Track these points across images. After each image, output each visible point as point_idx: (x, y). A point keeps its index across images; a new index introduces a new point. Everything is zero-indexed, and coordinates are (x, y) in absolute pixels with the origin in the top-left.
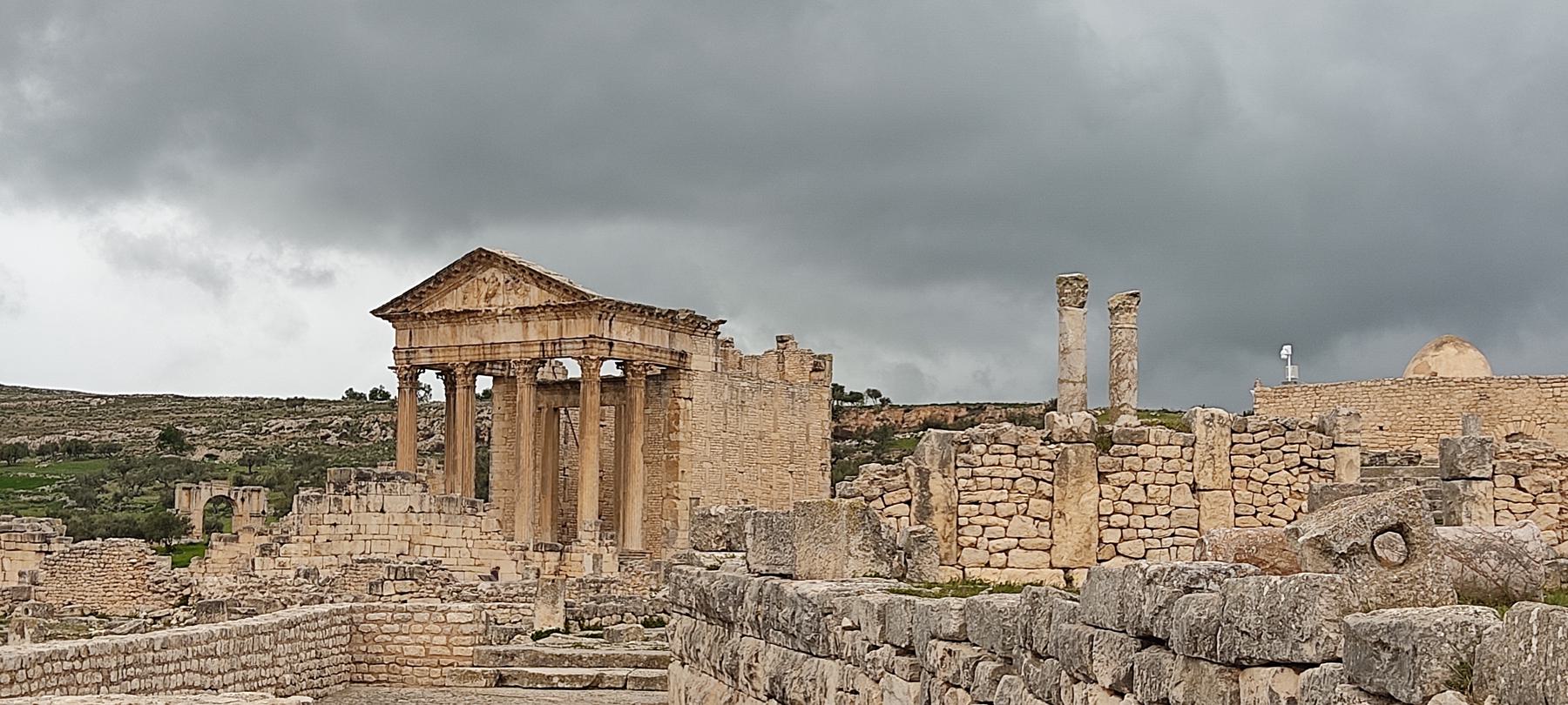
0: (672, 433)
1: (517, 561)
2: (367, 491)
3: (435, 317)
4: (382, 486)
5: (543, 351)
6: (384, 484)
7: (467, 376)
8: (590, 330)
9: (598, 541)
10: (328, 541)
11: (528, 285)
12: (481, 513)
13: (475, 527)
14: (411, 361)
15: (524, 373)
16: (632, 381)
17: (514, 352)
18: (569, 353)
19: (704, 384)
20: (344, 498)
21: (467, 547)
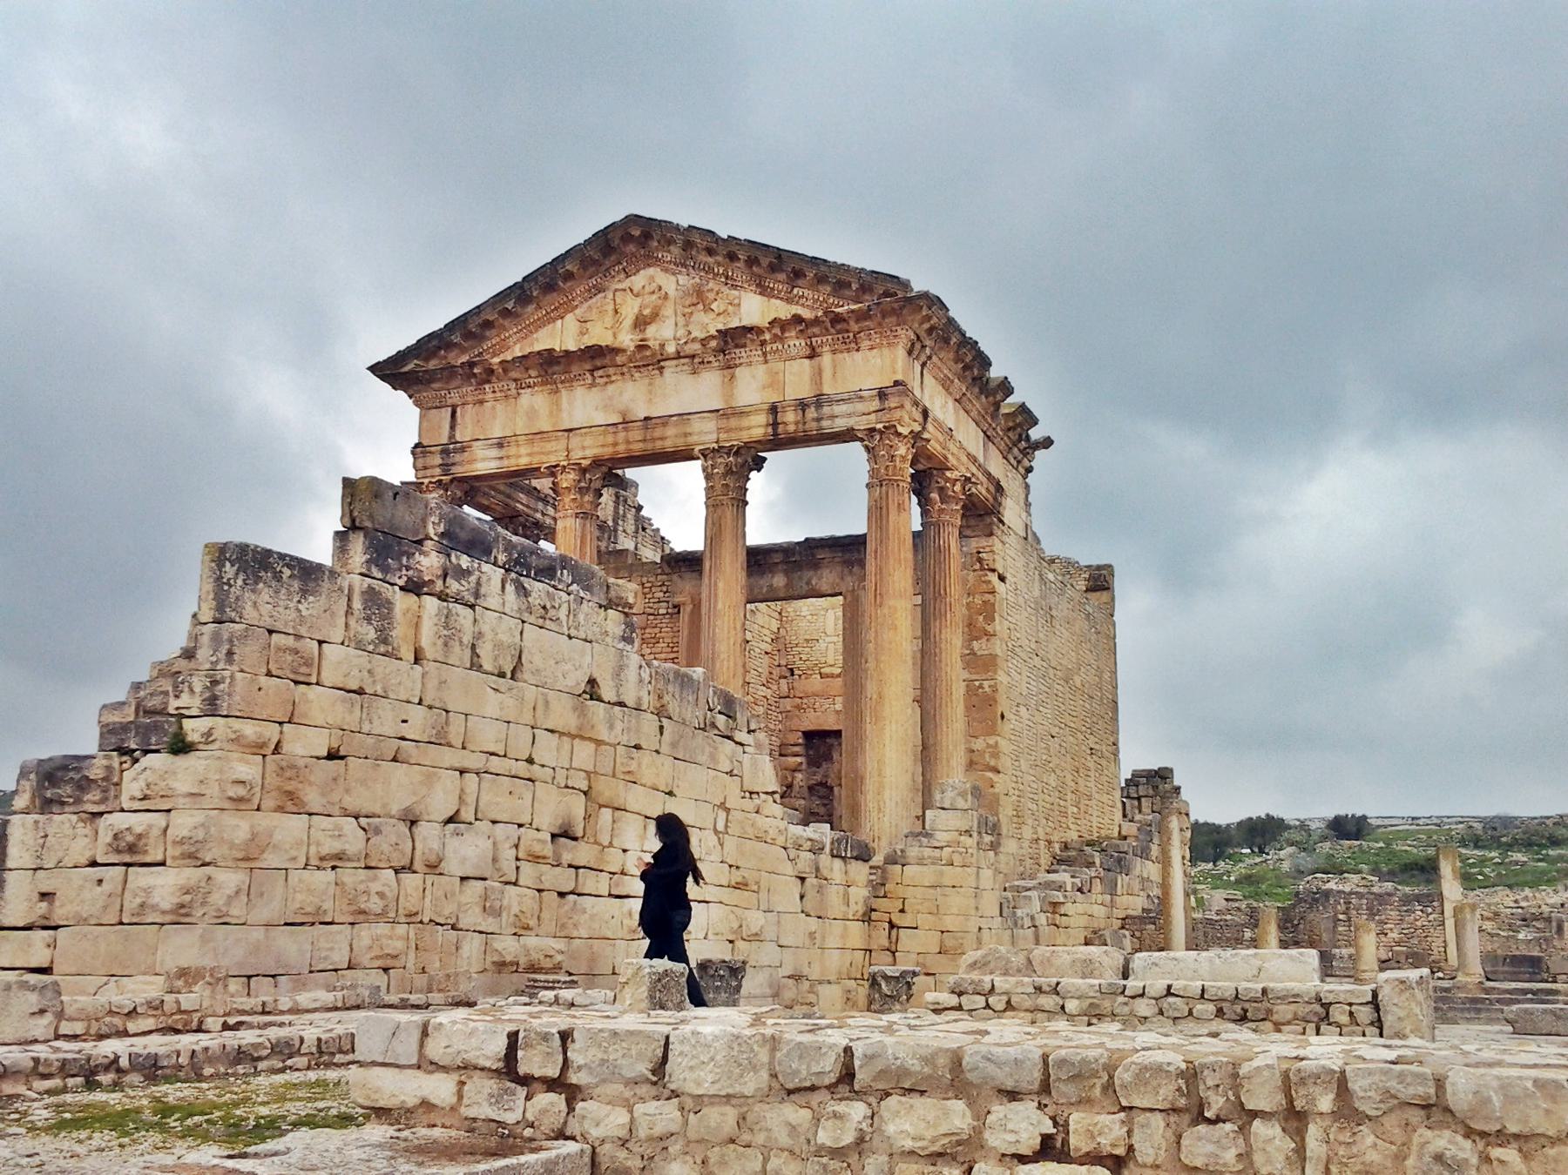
0: (977, 639)
1: (803, 879)
2: (477, 595)
3: (514, 374)
4: (523, 592)
5: (775, 424)
6: (527, 582)
7: (582, 491)
8: (894, 372)
9: (975, 834)
10: (333, 756)
11: (735, 293)
12: (741, 736)
13: (730, 773)
14: (454, 470)
15: (725, 475)
16: (941, 511)
17: (699, 433)
18: (840, 424)
19: (1016, 558)
20: (402, 603)
21: (716, 831)
